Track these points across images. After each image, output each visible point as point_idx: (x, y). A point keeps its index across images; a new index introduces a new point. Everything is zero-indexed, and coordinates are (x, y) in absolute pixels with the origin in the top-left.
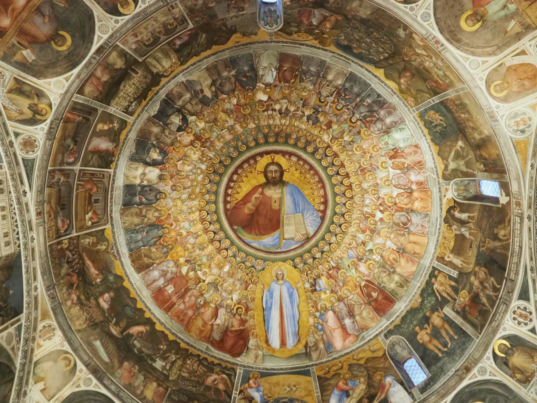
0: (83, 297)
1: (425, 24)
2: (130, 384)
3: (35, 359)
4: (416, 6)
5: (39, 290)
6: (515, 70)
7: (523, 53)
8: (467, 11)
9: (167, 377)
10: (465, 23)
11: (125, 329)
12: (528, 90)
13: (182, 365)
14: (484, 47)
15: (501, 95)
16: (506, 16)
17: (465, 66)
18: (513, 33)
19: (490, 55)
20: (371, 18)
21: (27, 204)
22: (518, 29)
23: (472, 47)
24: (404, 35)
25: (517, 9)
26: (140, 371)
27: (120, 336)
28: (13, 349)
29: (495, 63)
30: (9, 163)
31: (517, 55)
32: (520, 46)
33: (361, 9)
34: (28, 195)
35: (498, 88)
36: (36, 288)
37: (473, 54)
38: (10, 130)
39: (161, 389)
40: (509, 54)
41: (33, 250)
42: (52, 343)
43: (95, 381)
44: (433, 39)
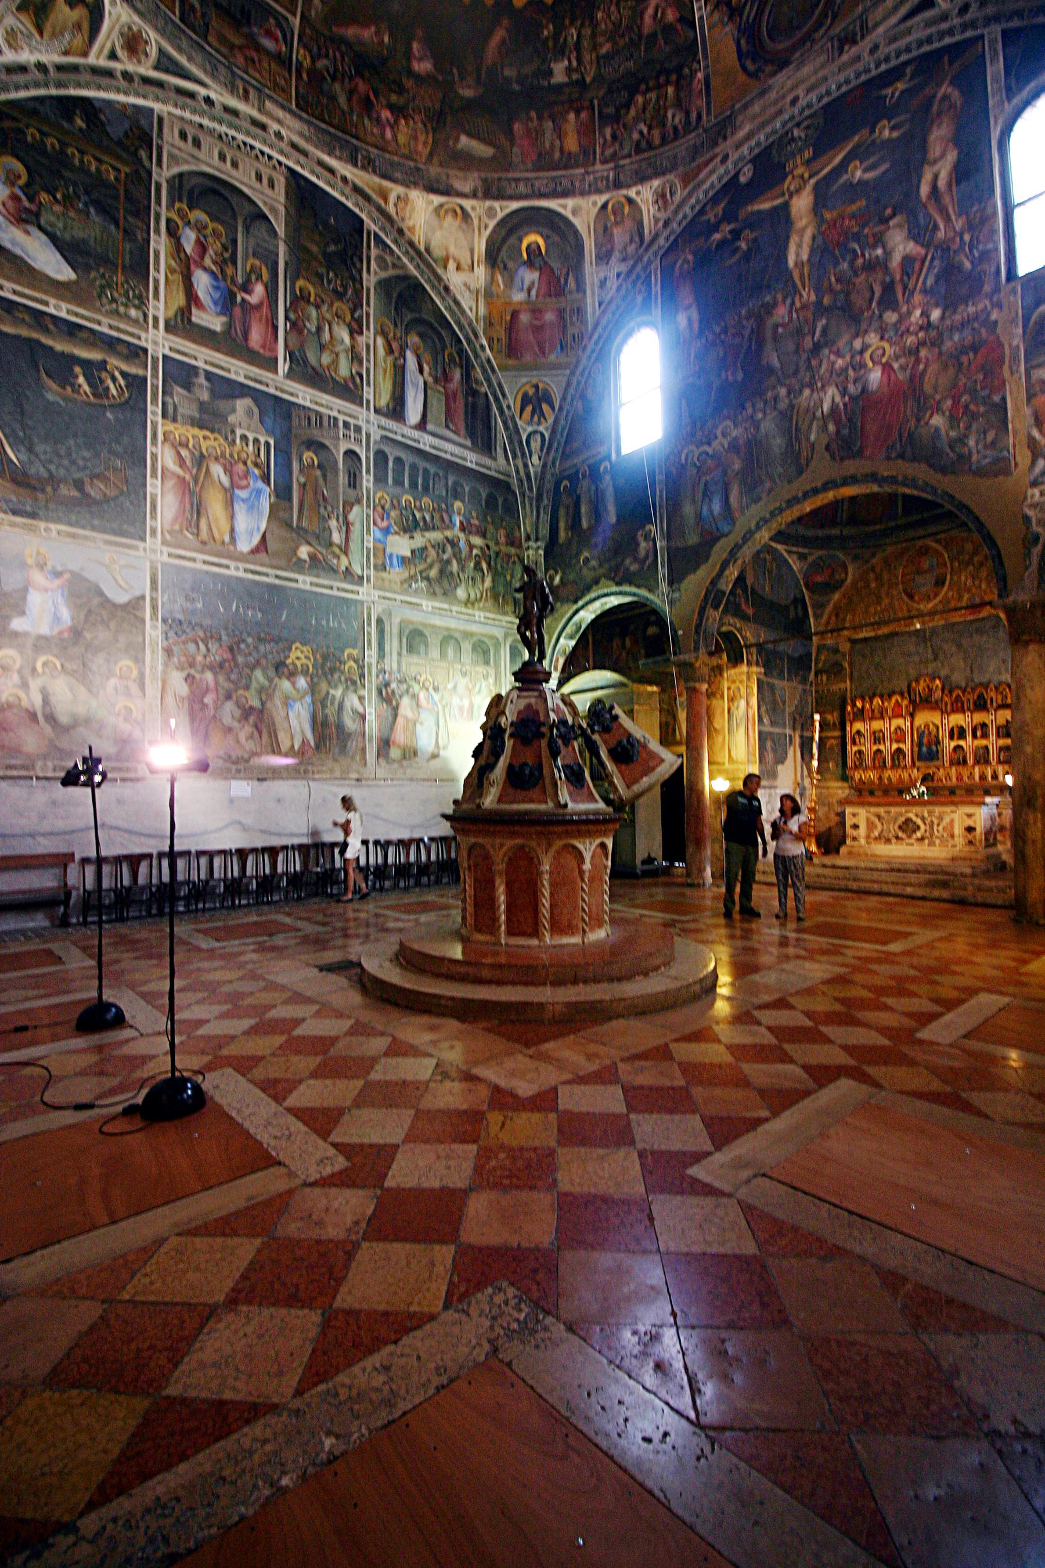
0: (394, 98)
2: (540, 155)
3: (422, 248)
5: (349, 176)
9: (581, 83)
11: (478, 69)
13: (594, 35)
21: (227, 109)
26: (540, 118)
27: (481, 90)
28: (394, 266)
30: (157, 99)
34: (213, 96)
36: (344, 179)
38: (103, 62)
39: (584, 115)
41: (294, 146)
42: (420, 212)
43: (497, 205)
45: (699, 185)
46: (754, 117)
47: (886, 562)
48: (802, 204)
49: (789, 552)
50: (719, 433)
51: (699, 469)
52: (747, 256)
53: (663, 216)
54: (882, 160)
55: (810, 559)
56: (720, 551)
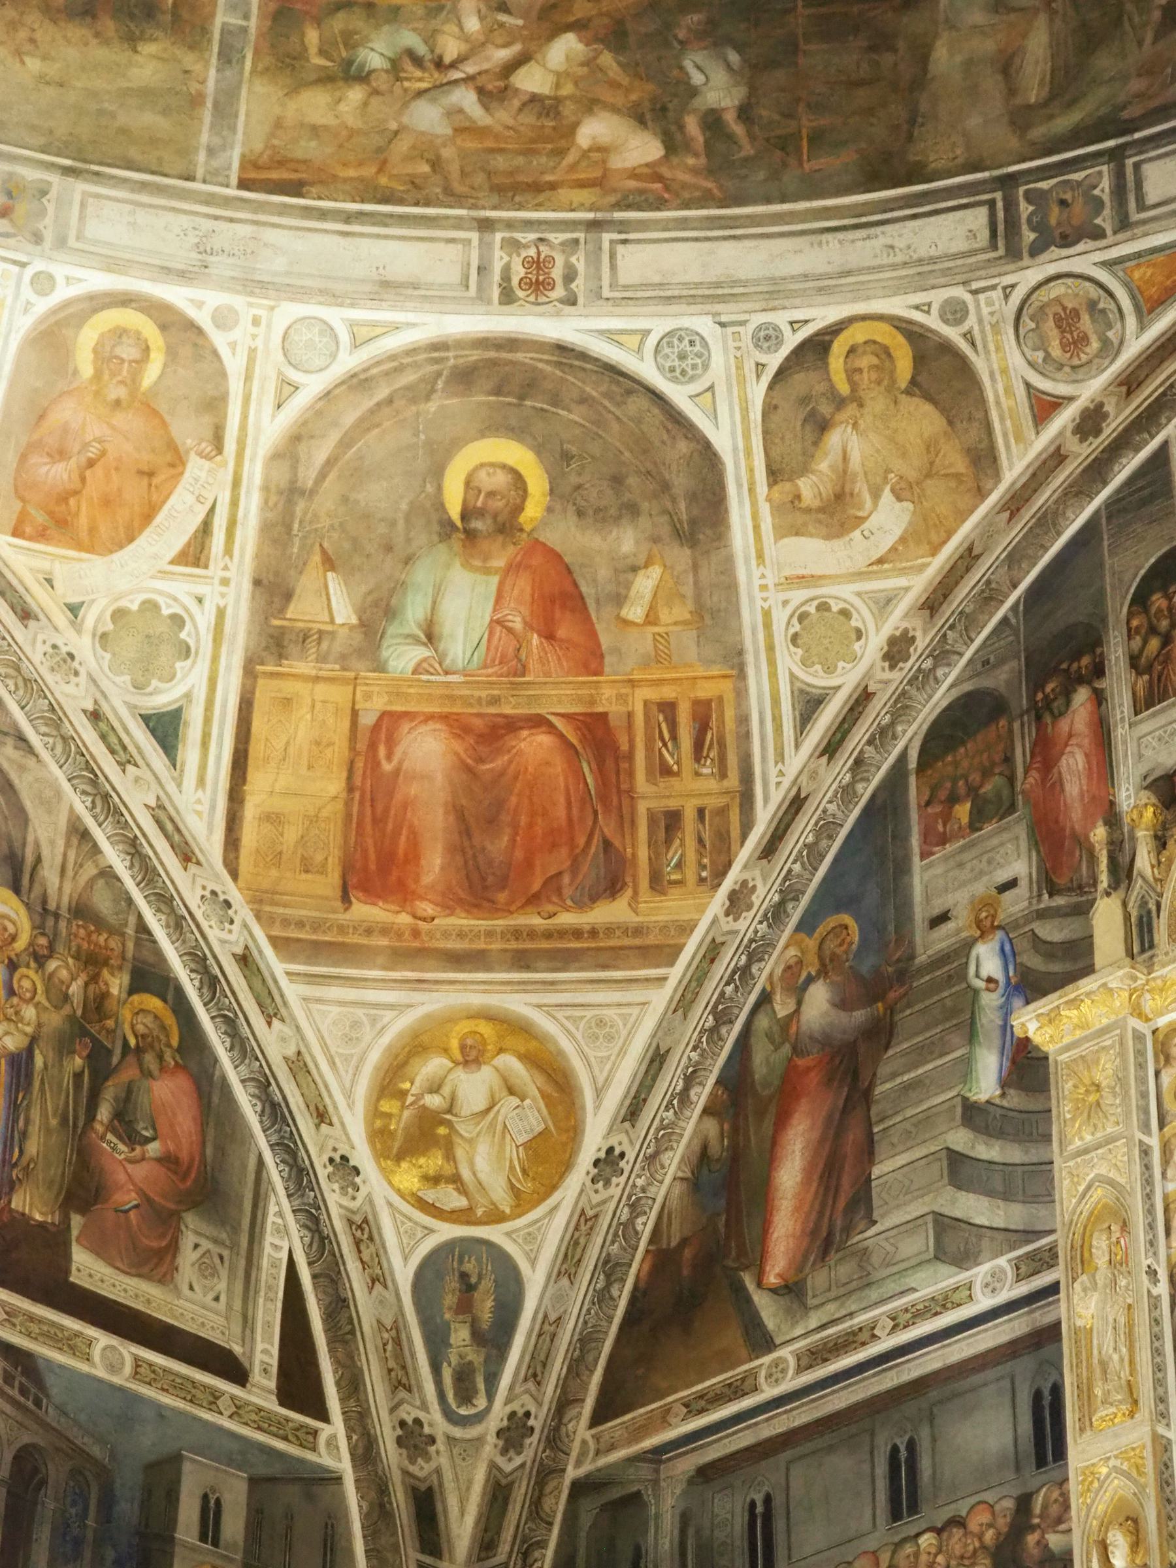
1: (659, 326)
4: (760, 367)
6: (151, 474)
7: (194, 554)
8: (550, 510)
10: (511, 462)
12: (23, 458)
14: (346, 443)
15: (88, 337)
16: (390, 612)
17: (334, 298)
18: (307, 583)
19: (297, 437)
20: (913, 23)
22: (303, 610)
23: (390, 401)
24: (697, 78)
25: (381, 667)
29: (243, 427)
31: (206, 528)
32: (233, 566)
33: (988, 46)
35: (128, 352)
37: (358, 382)
40: (234, 503)
44: (570, 276)
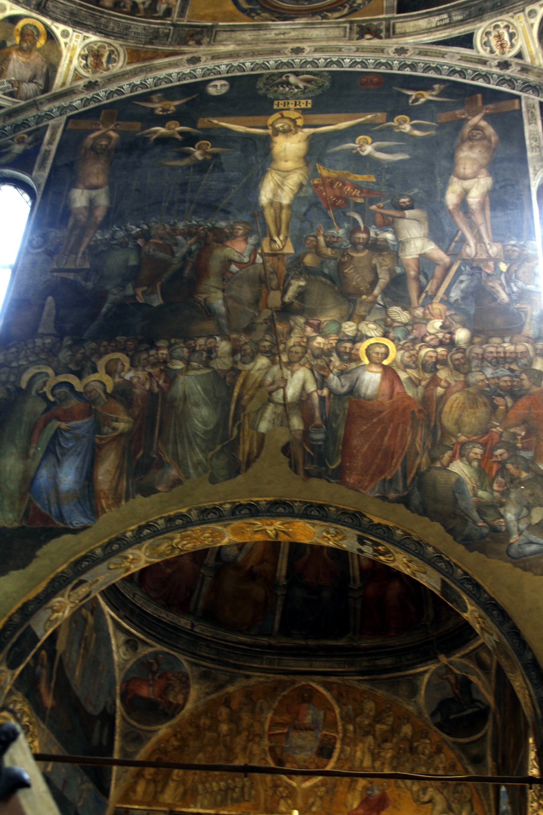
45: (151, 69)
46: (244, 42)
47: (249, 695)
48: (289, 147)
49: (118, 626)
50: (101, 364)
51: (50, 405)
52: (201, 167)
53: (88, 75)
54: (402, 152)
55: (143, 651)
56: (55, 556)
